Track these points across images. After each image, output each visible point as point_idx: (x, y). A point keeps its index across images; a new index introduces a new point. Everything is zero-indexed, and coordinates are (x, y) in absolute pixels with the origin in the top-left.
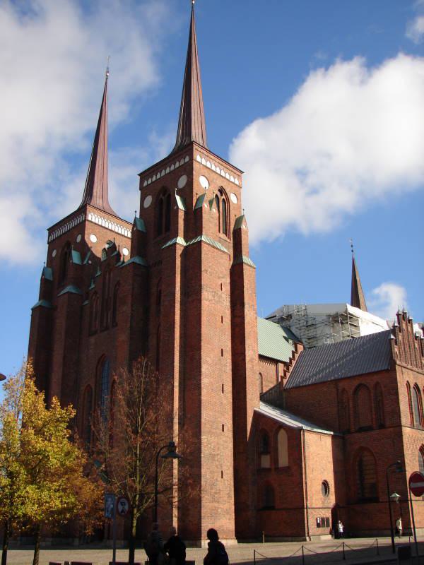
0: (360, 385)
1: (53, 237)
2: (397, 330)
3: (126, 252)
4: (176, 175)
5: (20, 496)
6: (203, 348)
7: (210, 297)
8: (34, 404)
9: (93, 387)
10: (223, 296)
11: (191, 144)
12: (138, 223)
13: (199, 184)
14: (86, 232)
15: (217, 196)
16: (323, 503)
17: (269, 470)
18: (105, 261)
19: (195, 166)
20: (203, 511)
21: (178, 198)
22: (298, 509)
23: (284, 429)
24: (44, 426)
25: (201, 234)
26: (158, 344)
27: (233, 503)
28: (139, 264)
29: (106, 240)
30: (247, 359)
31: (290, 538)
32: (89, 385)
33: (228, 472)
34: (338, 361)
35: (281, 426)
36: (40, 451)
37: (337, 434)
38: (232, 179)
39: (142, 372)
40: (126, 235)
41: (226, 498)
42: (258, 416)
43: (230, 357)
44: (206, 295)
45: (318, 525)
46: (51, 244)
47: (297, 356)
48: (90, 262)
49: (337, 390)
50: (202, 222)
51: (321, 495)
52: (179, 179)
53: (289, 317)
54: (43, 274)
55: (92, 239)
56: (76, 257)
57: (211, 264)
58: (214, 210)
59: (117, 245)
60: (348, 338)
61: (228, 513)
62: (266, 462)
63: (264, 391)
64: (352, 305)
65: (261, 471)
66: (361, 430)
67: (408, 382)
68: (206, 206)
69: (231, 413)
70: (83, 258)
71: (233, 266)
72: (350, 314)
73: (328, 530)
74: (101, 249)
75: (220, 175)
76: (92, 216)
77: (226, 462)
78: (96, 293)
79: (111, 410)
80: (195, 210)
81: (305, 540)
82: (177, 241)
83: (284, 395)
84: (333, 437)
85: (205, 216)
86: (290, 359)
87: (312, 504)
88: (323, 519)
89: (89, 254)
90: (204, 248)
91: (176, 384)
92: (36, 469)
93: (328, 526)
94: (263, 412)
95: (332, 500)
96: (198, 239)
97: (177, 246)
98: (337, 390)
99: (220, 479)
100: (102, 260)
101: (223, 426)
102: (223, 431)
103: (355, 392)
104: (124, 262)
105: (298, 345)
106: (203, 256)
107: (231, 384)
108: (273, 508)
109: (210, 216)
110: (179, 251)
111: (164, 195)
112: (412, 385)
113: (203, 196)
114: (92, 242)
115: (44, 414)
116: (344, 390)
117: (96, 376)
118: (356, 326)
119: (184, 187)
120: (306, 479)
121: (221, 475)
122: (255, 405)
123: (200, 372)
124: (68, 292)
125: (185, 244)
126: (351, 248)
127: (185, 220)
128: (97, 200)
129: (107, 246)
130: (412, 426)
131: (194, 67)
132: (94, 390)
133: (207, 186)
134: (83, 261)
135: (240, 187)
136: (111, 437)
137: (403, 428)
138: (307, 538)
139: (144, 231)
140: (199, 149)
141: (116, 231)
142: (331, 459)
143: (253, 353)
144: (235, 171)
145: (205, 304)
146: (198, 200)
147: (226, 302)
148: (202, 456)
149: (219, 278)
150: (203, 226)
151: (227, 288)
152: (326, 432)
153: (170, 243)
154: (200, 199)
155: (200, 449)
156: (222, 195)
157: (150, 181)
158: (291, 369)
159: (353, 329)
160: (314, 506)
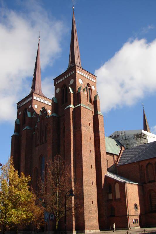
0: (148, 164)
1: (20, 106)
3: (49, 112)
4: (69, 79)
5: (9, 214)
6: (83, 150)
8: (14, 175)
9: (38, 168)
10: (90, 128)
11: (75, 66)
12: (54, 100)
14: (33, 104)
15: (86, 87)
16: (135, 213)
17: (112, 200)
18: (41, 115)
19: (77, 75)
20: (85, 218)
21: (70, 88)
22: (124, 216)
23: (118, 183)
24: (18, 184)
25: (80, 103)
26: (64, 149)
27: (98, 214)
28: (55, 116)
29: (41, 107)
30: (101, 154)
31: (122, 229)
32: (36, 167)
33: (95, 201)
34: (139, 153)
35: (116, 181)
36: (17, 195)
37: (140, 184)
38: (92, 80)
39: (58, 161)
40: (49, 104)
41: (94, 212)
42: (106, 177)
43: (94, 154)
44: (83, 128)
45: (133, 223)
46: (19, 110)
47: (122, 152)
48: (35, 116)
49: (139, 166)
50: (80, 98)
51: (134, 210)
52: (71, 80)
53: (118, 136)
54: (16, 122)
55: (36, 107)
56: (29, 114)
57: (85, 115)
58: (86, 93)
59: (46, 109)
60: (143, 144)
61: (96, 219)
62: (111, 197)
63: (109, 167)
64: (144, 130)
65: (109, 200)
66: (150, 182)
68: (82, 91)
69: (95, 177)
70: (32, 115)
71: (94, 116)
72: (143, 134)
73: (138, 224)
74: (39, 111)
75: (87, 78)
76: (35, 97)
77: (94, 197)
78: (38, 129)
79: (46, 177)
80: (78, 93)
81: (128, 229)
83: (117, 168)
84: (138, 185)
85: (82, 96)
86: (119, 154)
87: (130, 213)
88: (135, 220)
89: (34, 113)
90: (82, 109)
91: (72, 165)
92: (16, 203)
93: (138, 223)
94: (108, 176)
95: (139, 212)
96: (79, 105)
97: (71, 108)
98: (139, 166)
99: (92, 204)
100: (40, 115)
101: (92, 182)
102: (92, 184)
103: (147, 166)
104: (49, 116)
105: (122, 148)
106: (81, 112)
107: (95, 165)
108: (114, 216)
109: (84, 95)
110: (71, 110)
111: (64, 88)
113: (80, 87)
114: (35, 108)
115: (18, 180)
116: (142, 165)
117: (39, 163)
118: (146, 139)
119: (73, 84)
121: (92, 203)
122: (105, 173)
123: (82, 160)
124: (26, 129)
125: (74, 107)
127: (74, 97)
128: (36, 90)
129: (42, 109)
131: (75, 34)
132: (38, 169)
133: (82, 83)
135: (96, 83)
136: (46, 188)
138: (129, 228)
139: (57, 103)
140: (78, 68)
141: (45, 103)
142: (138, 195)
143: (103, 151)
145: (83, 132)
147: (92, 131)
148: (84, 195)
149: (88, 121)
151: (92, 125)
152: (135, 183)
153: (68, 107)
154: (79, 88)
155: (83, 192)
156: (88, 87)
157: (58, 82)
158: (120, 157)
159: (145, 140)
160: (131, 214)
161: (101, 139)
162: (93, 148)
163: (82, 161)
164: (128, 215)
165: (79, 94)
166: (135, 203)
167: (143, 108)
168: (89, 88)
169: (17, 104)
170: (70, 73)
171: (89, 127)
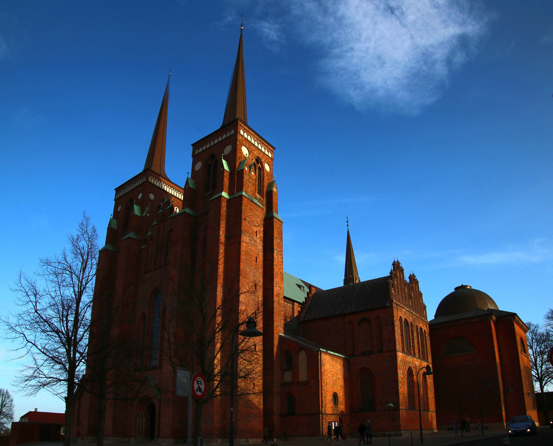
2: (394, 276)
7: (248, 241)
10: (258, 241)
12: (190, 182)
13: (241, 152)
21: (224, 162)
28: (190, 214)
30: (275, 293)
37: (346, 357)
44: (245, 238)
48: (148, 215)
54: (110, 224)
67: (400, 317)
82: (222, 195)
84: (344, 359)
85: (246, 177)
87: (325, 410)
90: (245, 201)
96: (239, 194)
109: (250, 177)
110: (224, 204)
112: (403, 320)
120: (322, 390)
122: (279, 331)
124: (130, 237)
126: (349, 223)
130: (403, 351)
134: (142, 213)
137: (397, 352)
139: (195, 189)
140: (243, 126)
144: (269, 146)
145: (244, 246)
146: (240, 162)
147: (260, 247)
150: (244, 184)
156: (258, 164)
157: (201, 150)
158: (307, 307)
161: (277, 265)
162: (261, 279)
163: (239, 303)
164: (322, 412)
165: (241, 173)
166: (334, 391)
167: (348, 225)
168: (259, 167)
169: (115, 191)
170: (226, 134)
171: (255, 238)
